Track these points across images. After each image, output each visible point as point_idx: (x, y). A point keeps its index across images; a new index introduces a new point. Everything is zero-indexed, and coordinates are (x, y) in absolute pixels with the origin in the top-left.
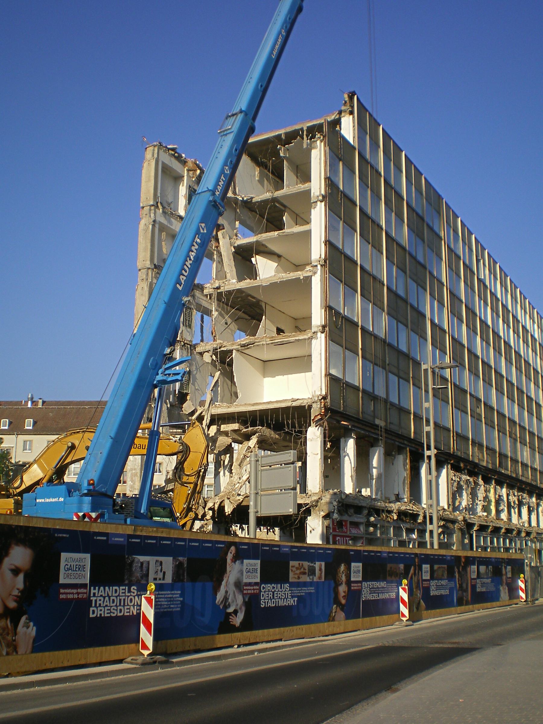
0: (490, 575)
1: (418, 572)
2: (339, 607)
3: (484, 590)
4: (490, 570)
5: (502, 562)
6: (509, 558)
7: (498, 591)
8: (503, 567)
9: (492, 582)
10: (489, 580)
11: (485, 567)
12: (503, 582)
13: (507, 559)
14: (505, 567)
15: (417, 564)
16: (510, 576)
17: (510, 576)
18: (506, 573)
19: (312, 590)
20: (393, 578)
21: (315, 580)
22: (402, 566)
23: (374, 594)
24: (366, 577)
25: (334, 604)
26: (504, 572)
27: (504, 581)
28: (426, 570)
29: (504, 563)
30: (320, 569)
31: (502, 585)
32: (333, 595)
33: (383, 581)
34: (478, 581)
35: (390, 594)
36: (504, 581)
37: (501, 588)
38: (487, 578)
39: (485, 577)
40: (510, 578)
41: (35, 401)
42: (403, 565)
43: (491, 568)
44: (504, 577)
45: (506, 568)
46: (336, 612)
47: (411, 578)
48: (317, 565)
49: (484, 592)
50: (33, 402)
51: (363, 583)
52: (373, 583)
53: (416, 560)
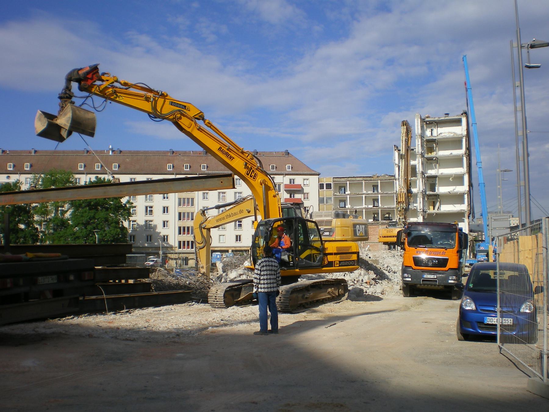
41: (114, 151)
50: (113, 151)
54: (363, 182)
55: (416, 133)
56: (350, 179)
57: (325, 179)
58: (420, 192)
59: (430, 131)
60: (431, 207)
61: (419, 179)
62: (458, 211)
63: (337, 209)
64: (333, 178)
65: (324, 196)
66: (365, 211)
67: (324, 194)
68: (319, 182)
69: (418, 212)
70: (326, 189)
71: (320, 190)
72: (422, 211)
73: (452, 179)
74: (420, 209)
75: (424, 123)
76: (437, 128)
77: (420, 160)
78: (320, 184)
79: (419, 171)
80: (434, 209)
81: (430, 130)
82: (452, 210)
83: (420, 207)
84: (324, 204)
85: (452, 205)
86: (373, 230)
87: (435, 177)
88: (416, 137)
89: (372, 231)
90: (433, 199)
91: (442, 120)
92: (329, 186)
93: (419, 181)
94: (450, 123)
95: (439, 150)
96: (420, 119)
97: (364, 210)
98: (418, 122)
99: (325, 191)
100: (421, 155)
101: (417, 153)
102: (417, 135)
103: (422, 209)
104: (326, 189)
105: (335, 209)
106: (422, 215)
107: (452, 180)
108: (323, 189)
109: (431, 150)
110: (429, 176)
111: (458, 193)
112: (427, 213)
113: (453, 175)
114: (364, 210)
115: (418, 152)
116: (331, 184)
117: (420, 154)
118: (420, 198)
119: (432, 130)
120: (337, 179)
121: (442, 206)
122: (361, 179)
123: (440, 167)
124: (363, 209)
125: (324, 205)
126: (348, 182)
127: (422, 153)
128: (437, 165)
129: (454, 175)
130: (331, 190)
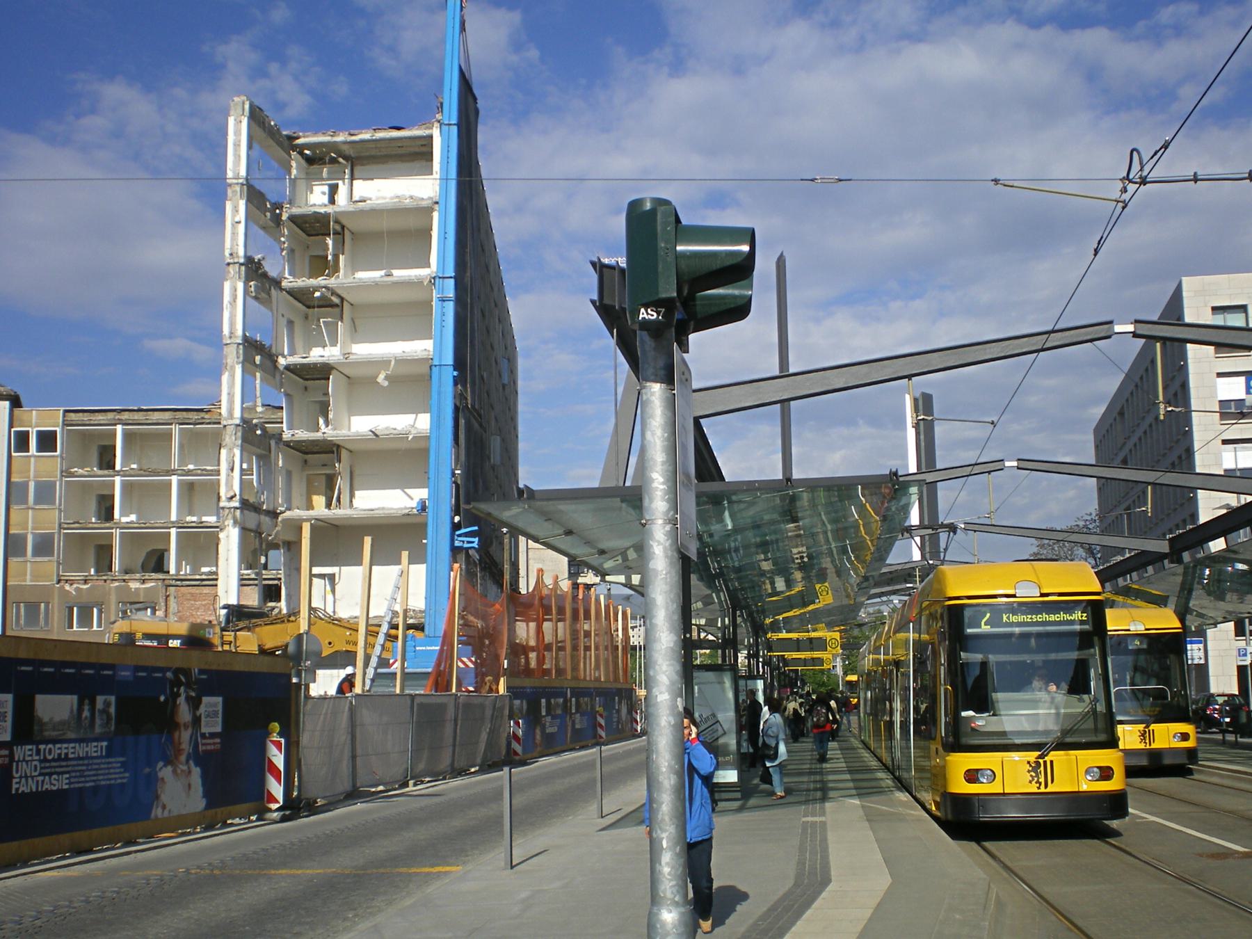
0: (98, 730)
3: (59, 783)
4: (105, 711)
5: (179, 684)
6: (214, 667)
7: (152, 782)
8: (181, 700)
9: (110, 752)
10: (95, 749)
11: (75, 698)
12: (179, 751)
13: (201, 671)
14: (188, 699)
16: (218, 729)
17: (218, 729)
18: (197, 721)
26: (184, 713)
27: (186, 746)
28: (211, 709)
29: (188, 685)
31: (168, 762)
34: (19, 752)
36: (186, 746)
37: (166, 772)
38: (79, 741)
39: (71, 735)
40: (213, 735)
43: (107, 704)
44: (185, 736)
45: (195, 703)
49: (61, 792)
54: (176, 429)
55: (230, 174)
56: (125, 416)
57: (37, 415)
58: (230, 422)
59: (324, 193)
60: (319, 501)
61: (233, 368)
62: (407, 511)
63: (77, 525)
64: (66, 411)
65: (29, 477)
66: (178, 533)
67: (29, 471)
68: (11, 426)
69: (223, 508)
70: (38, 451)
71: (13, 454)
72: (237, 504)
73: (387, 378)
74: (232, 498)
75: (294, 154)
76: (352, 178)
77: (240, 286)
78: (16, 432)
79: (232, 334)
80: (328, 506)
81: (326, 189)
82: (383, 508)
83: (229, 485)
84: (23, 507)
85: (398, 492)
86: (204, 605)
87: (322, 372)
88: (229, 191)
89: (198, 608)
90: (324, 465)
91: (362, 141)
92: (47, 441)
93: (232, 376)
94: (403, 161)
95: (354, 267)
96: (246, 119)
97: (173, 531)
98: (240, 131)
99: (32, 460)
100: (243, 268)
101: (229, 261)
102: (230, 185)
103: (238, 497)
104: (38, 451)
105: (66, 526)
106: (235, 522)
107: (386, 384)
108: (28, 452)
109: (321, 265)
110: (296, 365)
111: (411, 437)
112: (280, 519)
113: (391, 361)
114: (173, 531)
115: (231, 254)
116: (56, 431)
117: (241, 264)
118: (231, 450)
119: (333, 190)
120: (81, 414)
121: (357, 493)
122: (167, 415)
123: (356, 334)
124: (170, 528)
125: (28, 508)
126: (119, 428)
127: (249, 261)
128: (340, 323)
129: (393, 363)
130: (57, 456)
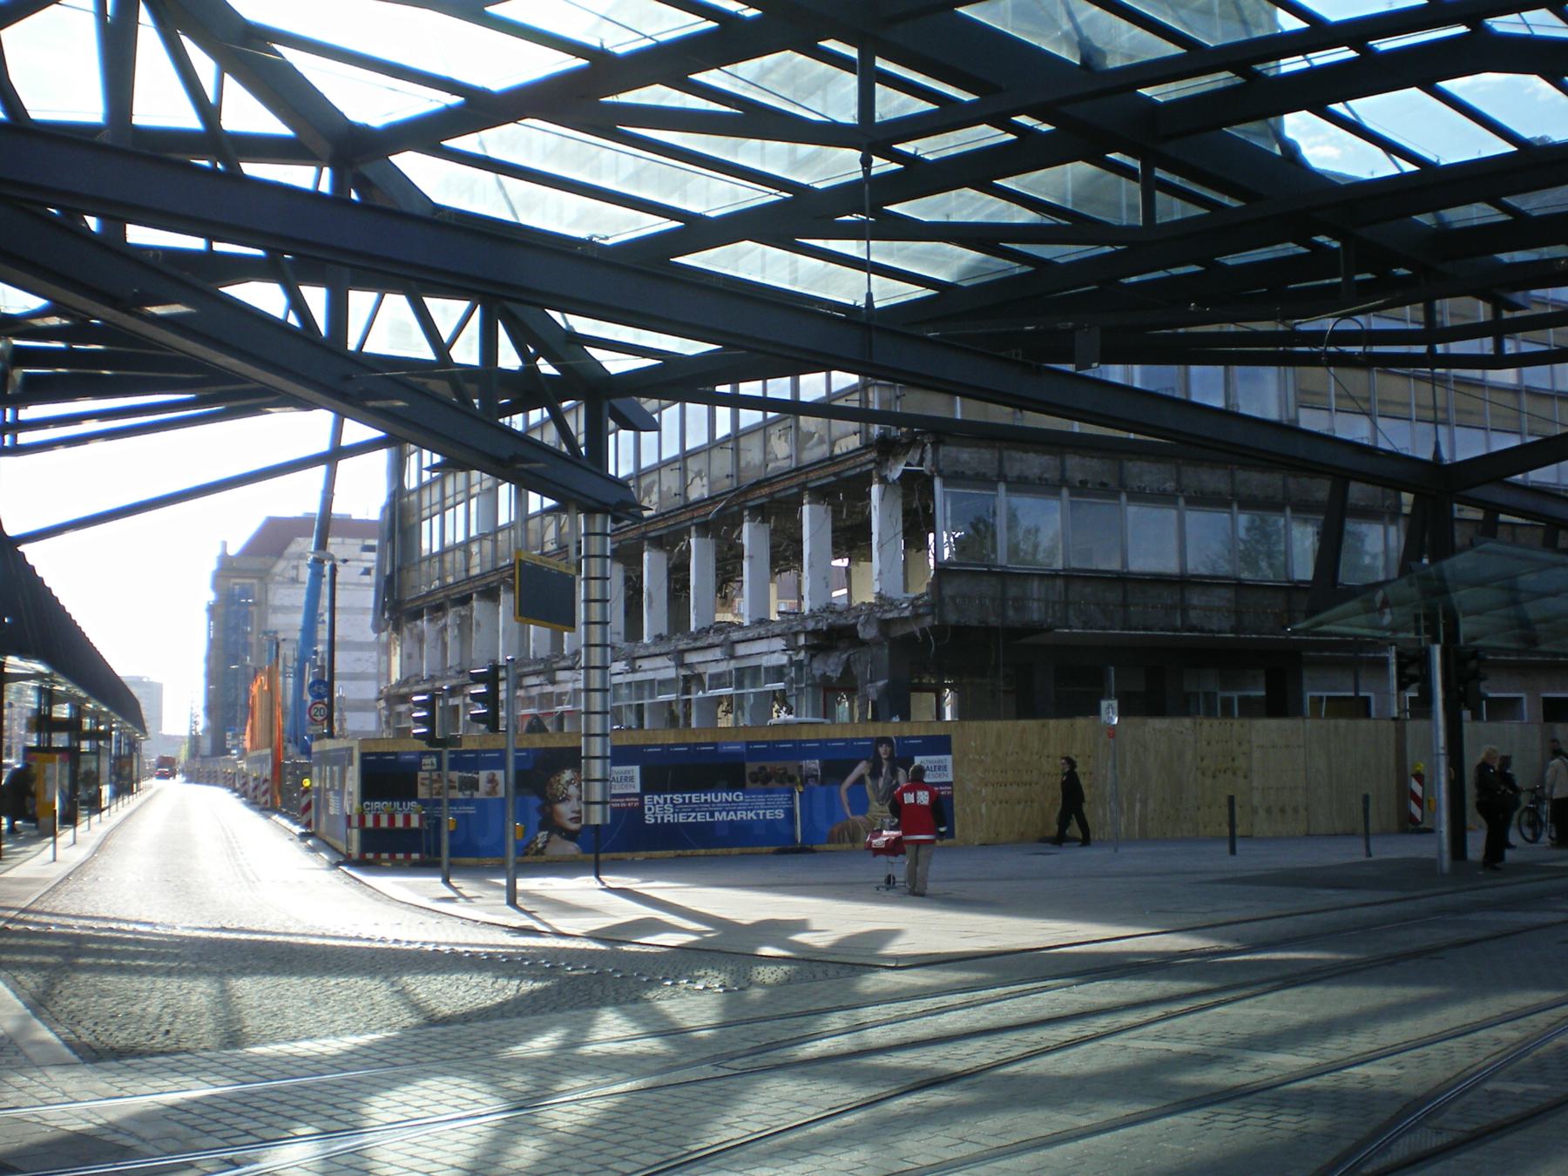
1: (894, 773)
2: (560, 834)
15: (884, 756)
19: (471, 810)
20: (773, 784)
21: (477, 795)
22: (813, 765)
23: (694, 814)
24: (652, 784)
25: (542, 828)
30: (492, 780)
32: (536, 818)
33: (732, 788)
35: (761, 812)
42: (817, 761)
46: (547, 841)
47: (860, 780)
48: (483, 776)
51: (646, 797)
52: (687, 796)
53: (882, 750)
